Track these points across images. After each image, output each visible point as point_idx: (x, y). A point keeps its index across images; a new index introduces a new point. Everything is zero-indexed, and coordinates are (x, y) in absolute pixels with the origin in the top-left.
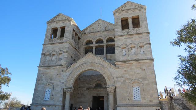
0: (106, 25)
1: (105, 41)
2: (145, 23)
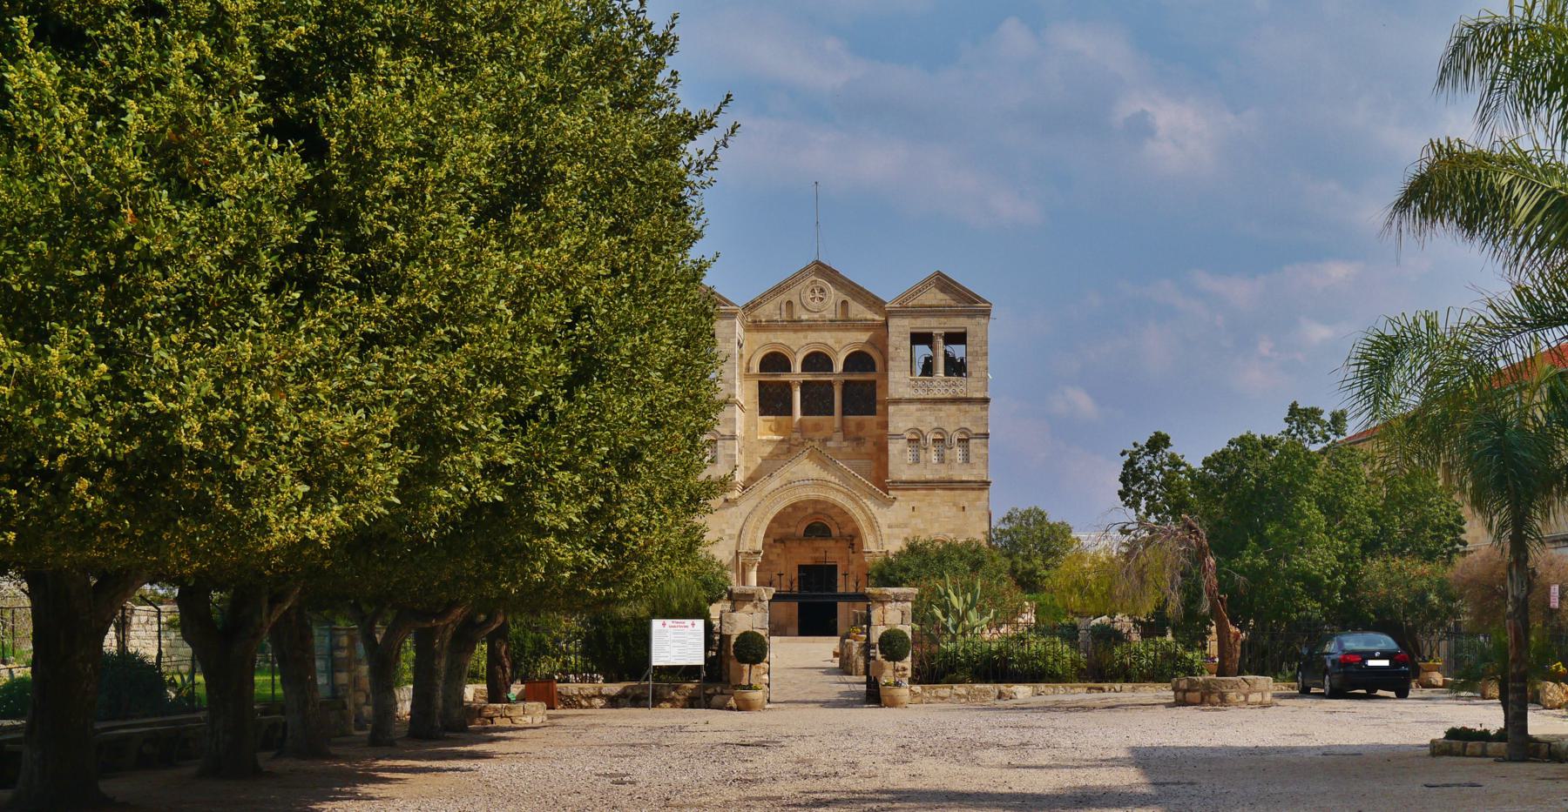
1: (839, 366)
2: (980, 363)
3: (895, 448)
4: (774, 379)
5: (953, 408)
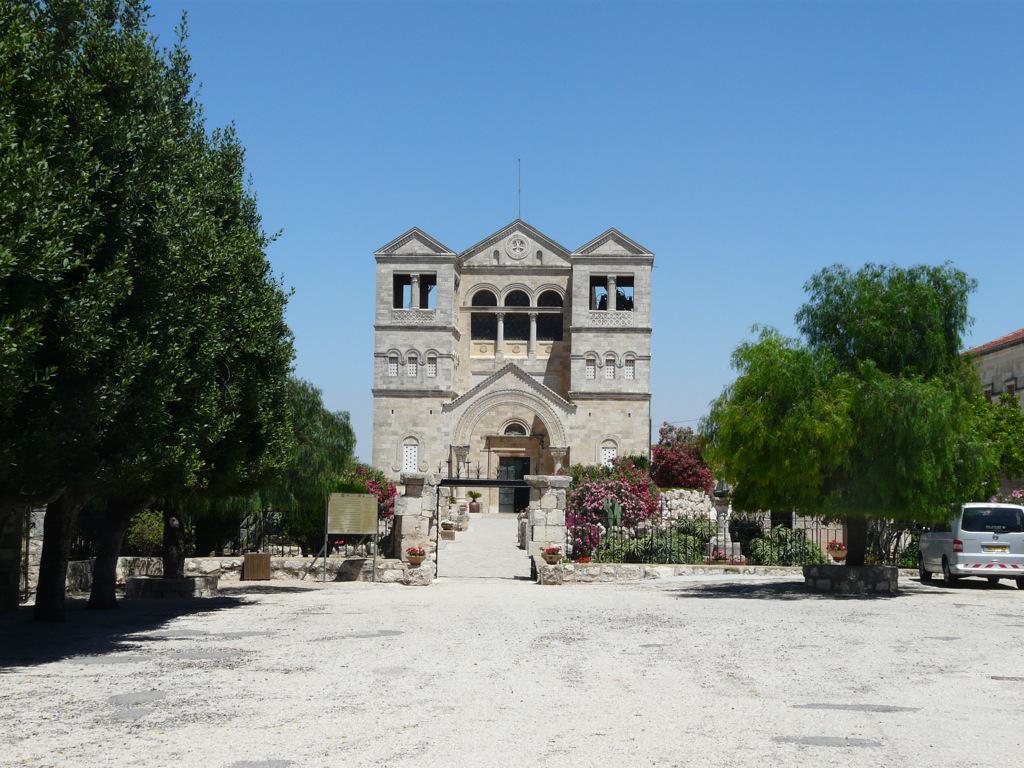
1: (534, 303)
2: (644, 301)
3: (576, 366)
5: (622, 336)
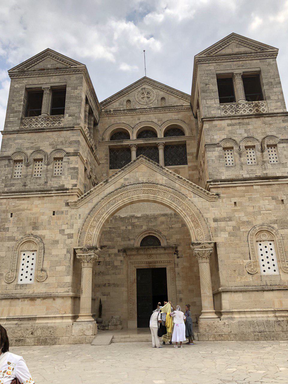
0: (162, 94)
3: (213, 155)
4: (119, 144)
